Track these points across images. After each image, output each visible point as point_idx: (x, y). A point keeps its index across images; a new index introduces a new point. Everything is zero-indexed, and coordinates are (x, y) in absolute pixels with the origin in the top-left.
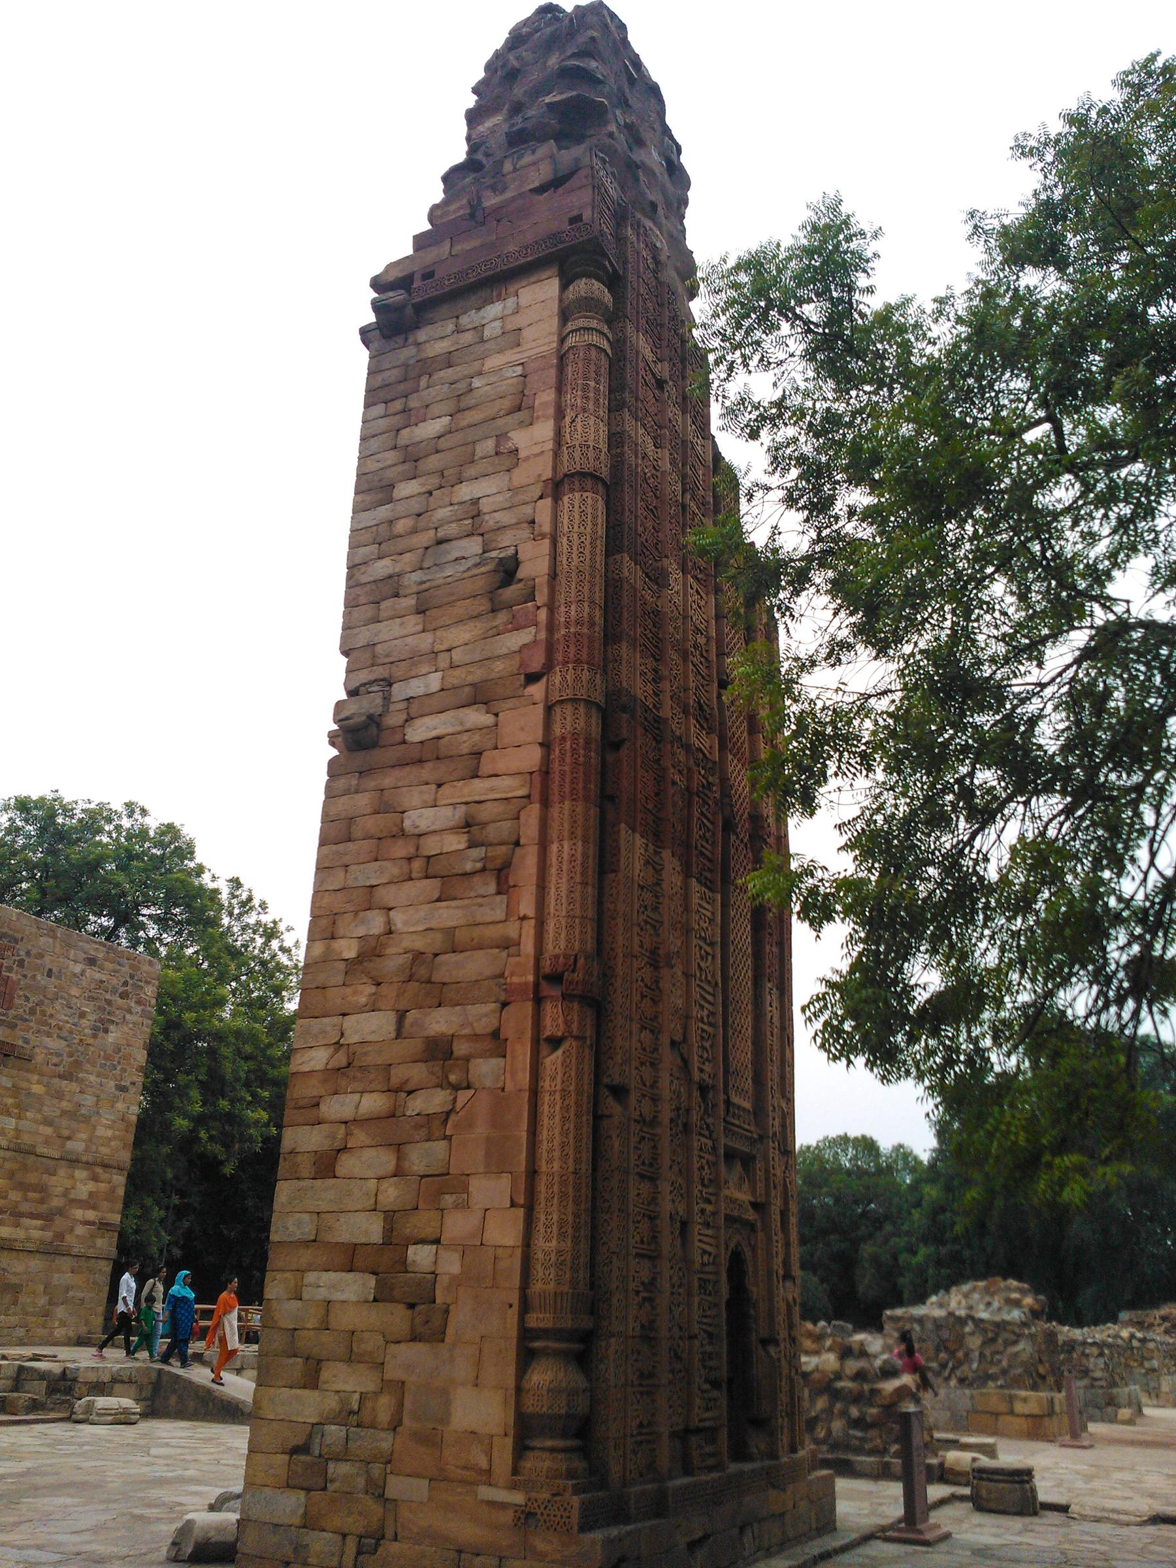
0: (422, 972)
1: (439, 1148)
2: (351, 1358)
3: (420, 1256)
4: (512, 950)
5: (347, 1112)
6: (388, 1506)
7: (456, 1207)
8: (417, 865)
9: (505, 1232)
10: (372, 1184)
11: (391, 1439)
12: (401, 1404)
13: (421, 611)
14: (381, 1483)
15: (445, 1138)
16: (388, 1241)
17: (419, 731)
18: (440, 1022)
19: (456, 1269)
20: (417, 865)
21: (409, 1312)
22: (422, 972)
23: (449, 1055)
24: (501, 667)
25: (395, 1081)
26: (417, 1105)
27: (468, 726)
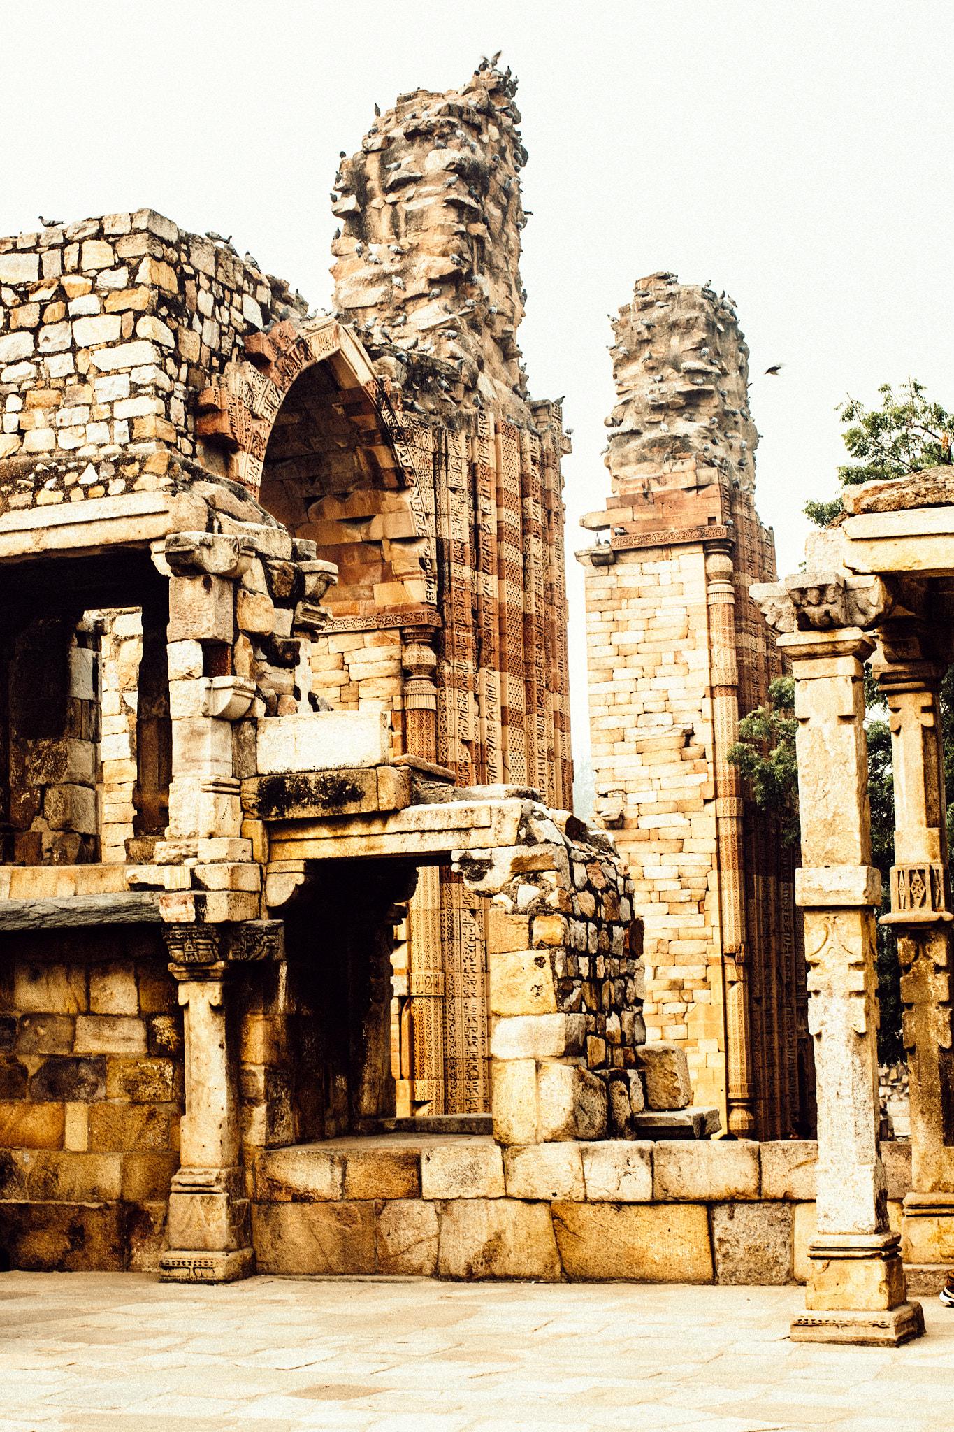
0: (663, 949)
8: (654, 896)
18: (676, 973)
22: (663, 949)
23: (682, 988)
25: (656, 999)
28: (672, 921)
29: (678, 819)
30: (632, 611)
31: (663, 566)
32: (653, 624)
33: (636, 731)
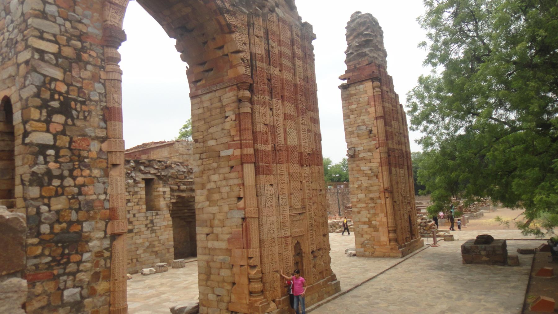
1: (374, 210)
2: (367, 234)
9: (384, 220)
17: (361, 155)
18: (371, 195)
28: (370, 182)
29: (370, 154)
30: (354, 99)
31: (361, 86)
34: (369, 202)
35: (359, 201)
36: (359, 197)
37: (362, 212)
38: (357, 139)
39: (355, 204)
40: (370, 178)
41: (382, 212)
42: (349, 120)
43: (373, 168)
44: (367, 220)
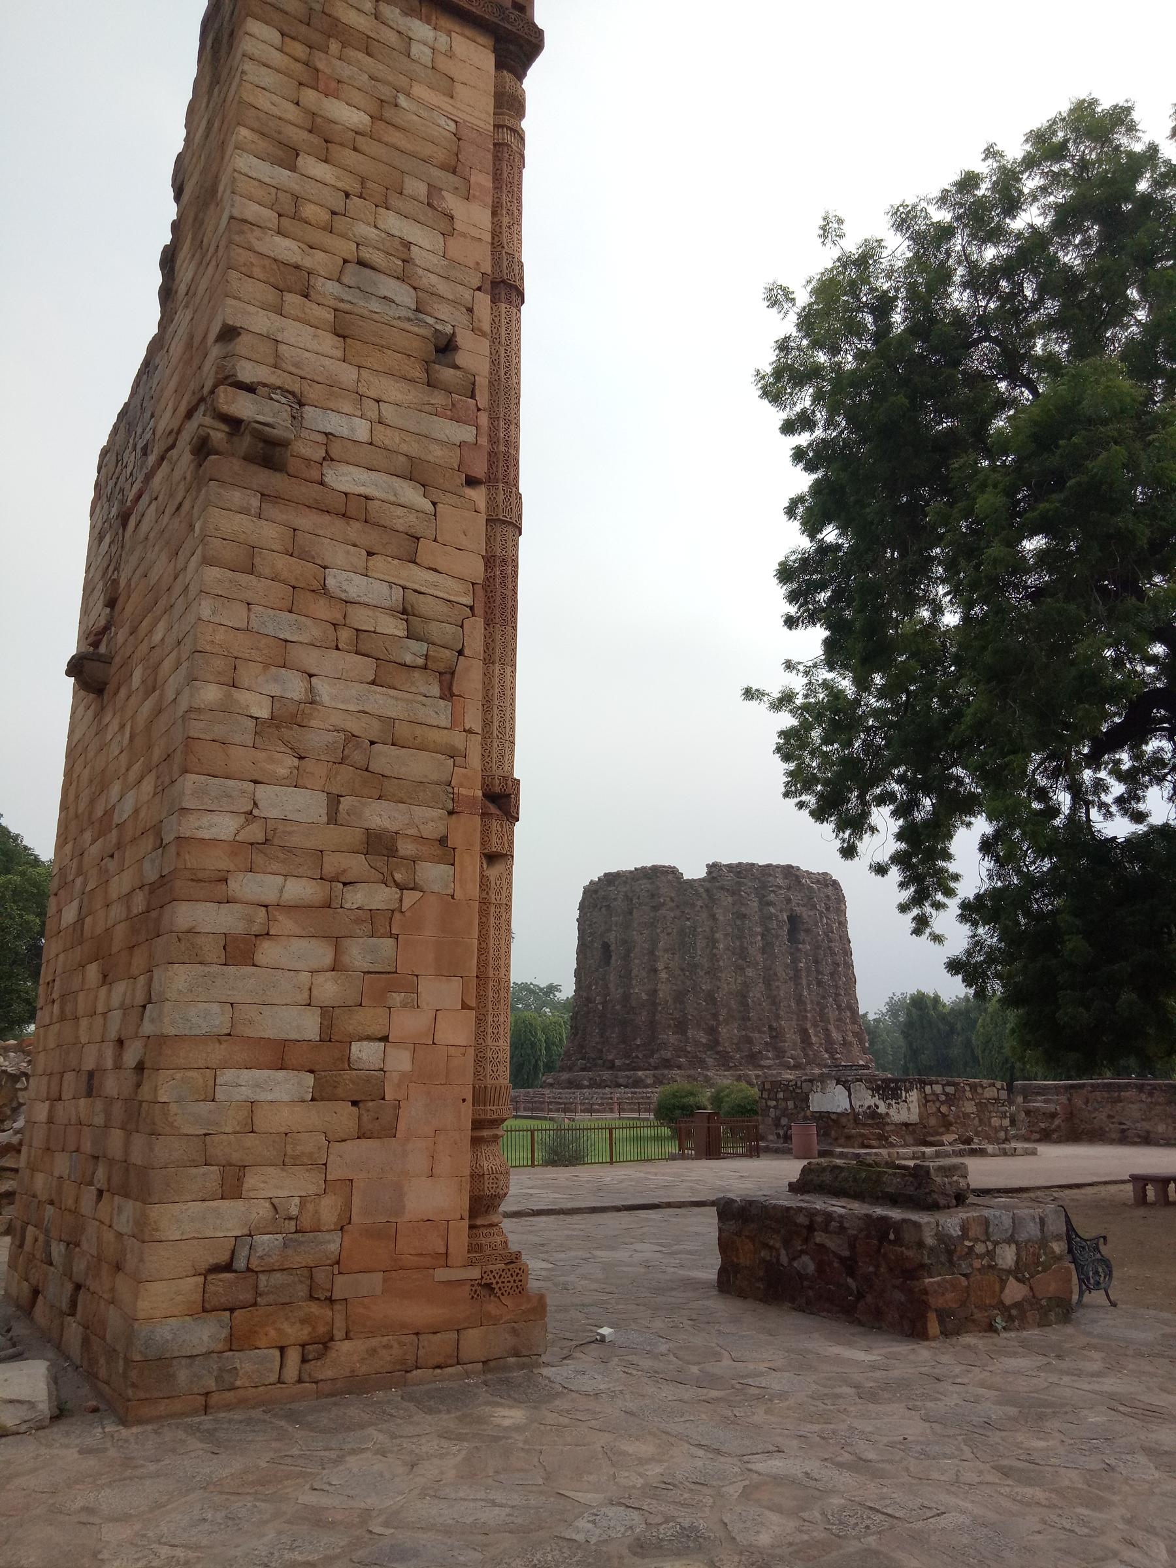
0: (357, 757)
3: (366, 1053)
4: (459, 760)
5: (270, 897)
6: (337, 1307)
7: (405, 1006)
8: (345, 635)
10: (305, 977)
11: (339, 1240)
12: (349, 1204)
13: (340, 333)
14: (328, 1286)
15: (391, 936)
16: (327, 1037)
17: (347, 479)
18: (381, 816)
19: (406, 1066)
20: (345, 635)
21: (355, 1109)
22: (357, 757)
23: (392, 852)
24: (439, 453)
25: (329, 869)
26: (357, 898)
27: (402, 500)
28: (383, 702)
29: (411, 494)
31: (420, 30)
32: (389, 113)
33: (332, 287)
34: (357, 864)
35: (264, 846)
36: (268, 810)
37: (268, 952)
38: (329, 343)
39: (217, 861)
40: (386, 671)
41: (446, 968)
42: (283, 176)
43: (426, 606)
44: (308, 1026)
